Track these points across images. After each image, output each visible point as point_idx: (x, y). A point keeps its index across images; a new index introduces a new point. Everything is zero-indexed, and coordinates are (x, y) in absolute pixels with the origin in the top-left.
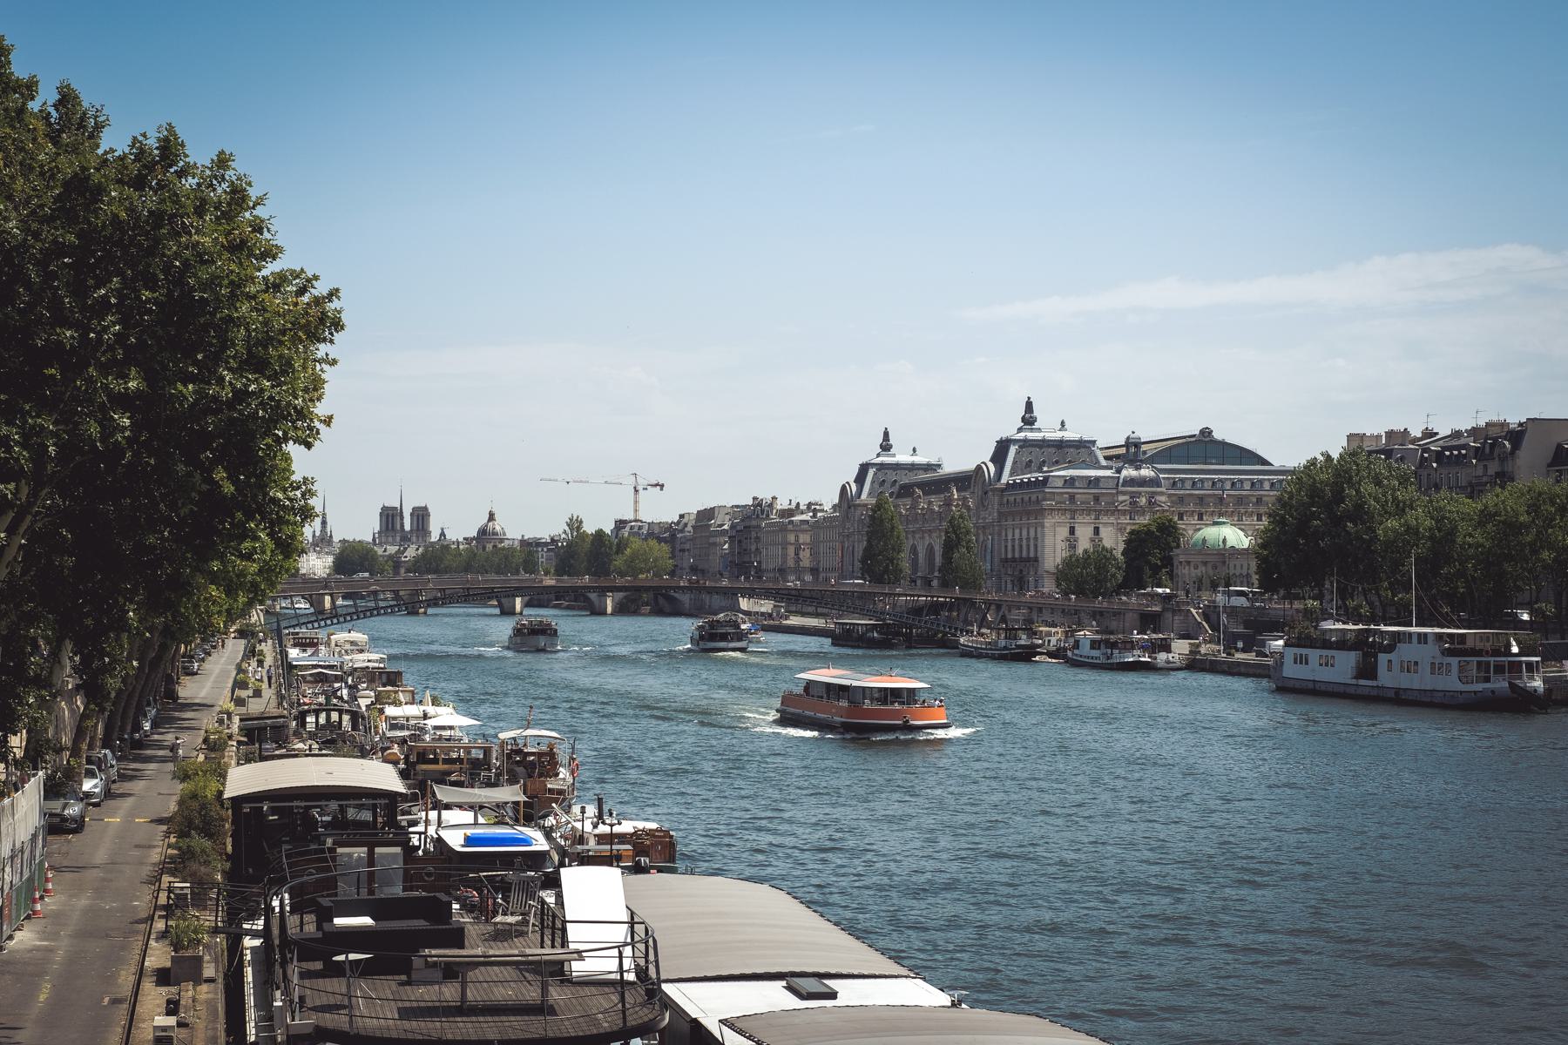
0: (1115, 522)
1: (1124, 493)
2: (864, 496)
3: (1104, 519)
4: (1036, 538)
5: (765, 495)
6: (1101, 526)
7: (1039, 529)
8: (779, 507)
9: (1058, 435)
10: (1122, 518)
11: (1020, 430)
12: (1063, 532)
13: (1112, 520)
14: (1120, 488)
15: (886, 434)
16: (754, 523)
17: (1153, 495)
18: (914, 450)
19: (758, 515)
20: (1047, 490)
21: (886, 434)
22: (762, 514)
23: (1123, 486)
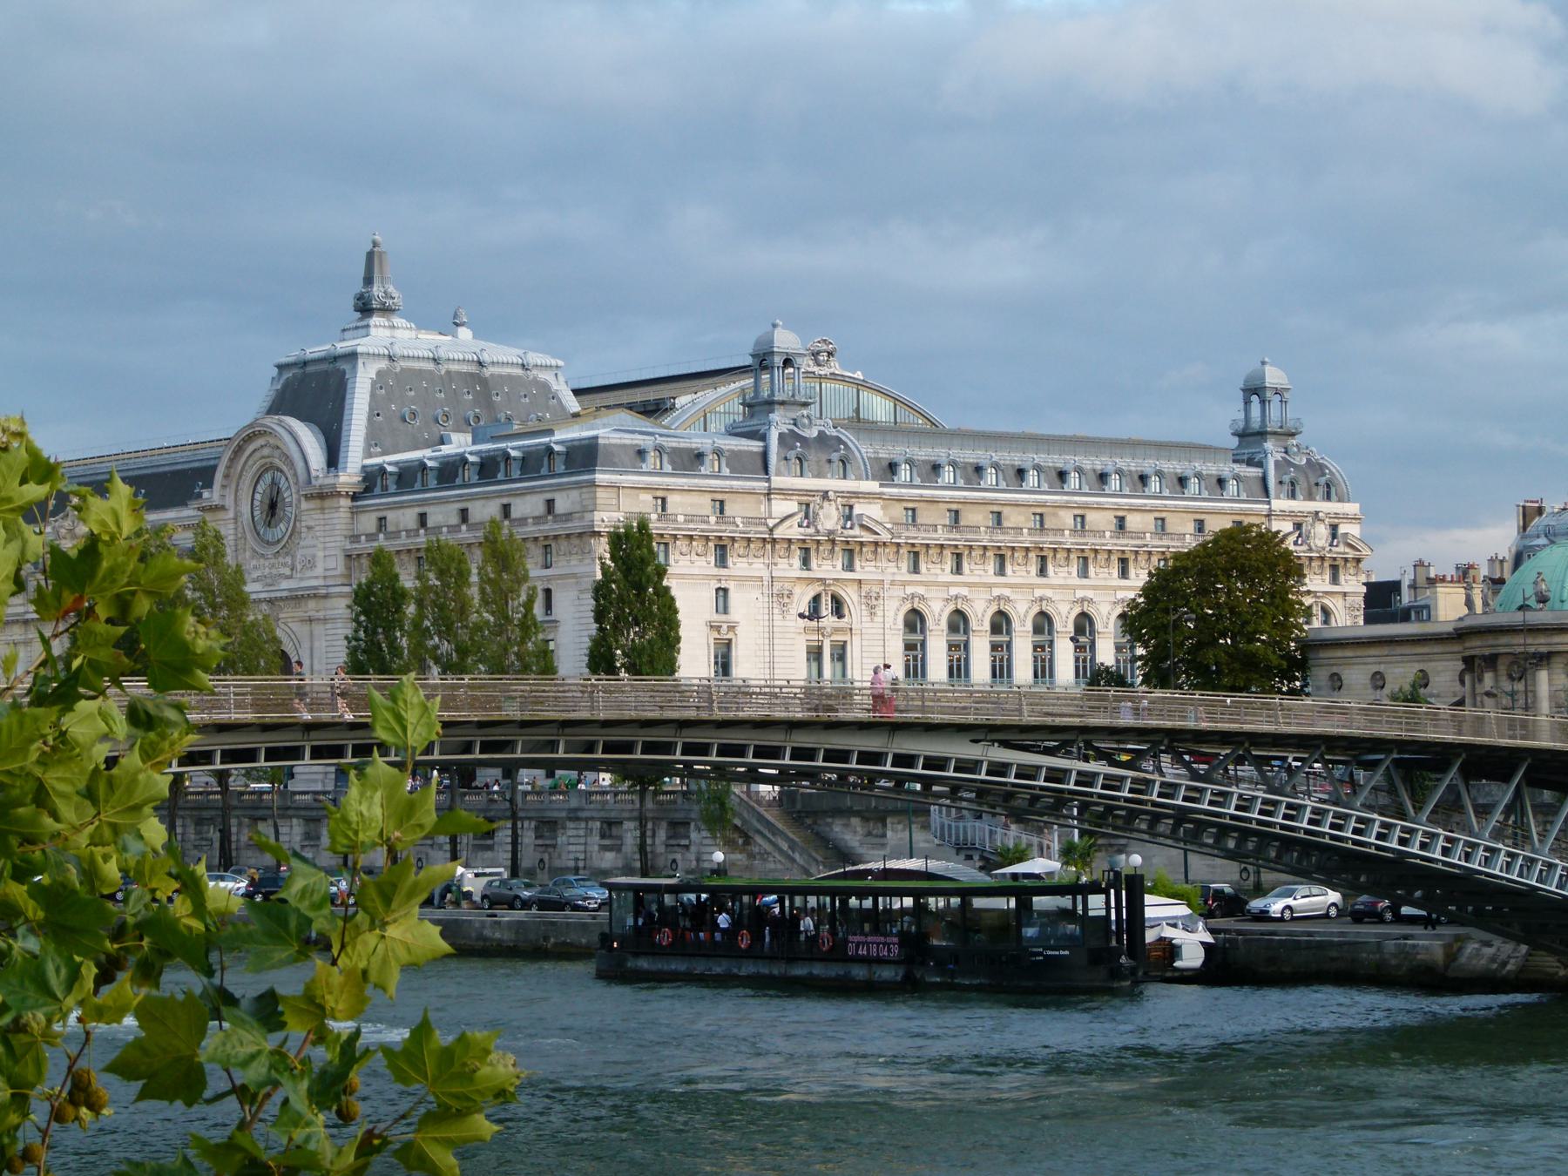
0: (765, 574)
1: (785, 493)
6: (731, 585)
10: (783, 563)
13: (758, 567)
14: (778, 481)
23: (777, 475)
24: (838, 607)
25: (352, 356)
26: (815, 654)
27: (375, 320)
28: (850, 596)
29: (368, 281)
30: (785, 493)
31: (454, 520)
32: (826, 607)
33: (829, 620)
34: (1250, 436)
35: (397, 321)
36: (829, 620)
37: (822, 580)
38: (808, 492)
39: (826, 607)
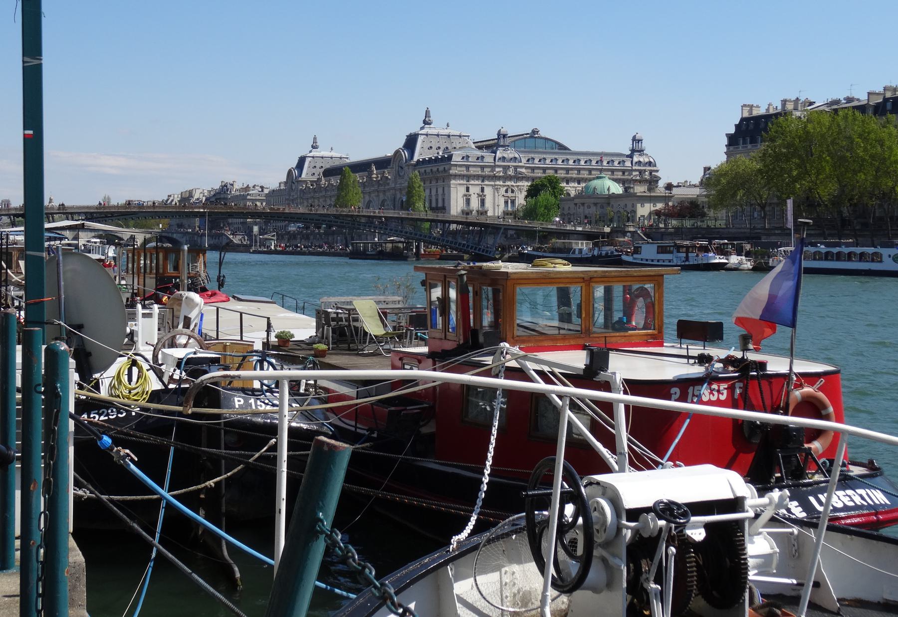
1: (499, 166)
2: (303, 176)
3: (487, 182)
4: (444, 194)
5: (228, 180)
7: (446, 189)
8: (238, 188)
9: (446, 132)
11: (422, 128)
12: (462, 190)
14: (497, 163)
15: (315, 138)
16: (222, 196)
17: (516, 167)
18: (332, 149)
19: (225, 192)
20: (452, 163)
21: (315, 138)
22: (227, 191)
23: (498, 161)
24: (513, 191)
25: (418, 134)
26: (506, 202)
27: (426, 126)
28: (516, 189)
29: (426, 117)
30: (499, 166)
31: (430, 171)
32: (510, 190)
33: (510, 194)
34: (633, 151)
35: (431, 126)
36: (510, 194)
37: (508, 186)
38: (505, 166)
39: (510, 190)
